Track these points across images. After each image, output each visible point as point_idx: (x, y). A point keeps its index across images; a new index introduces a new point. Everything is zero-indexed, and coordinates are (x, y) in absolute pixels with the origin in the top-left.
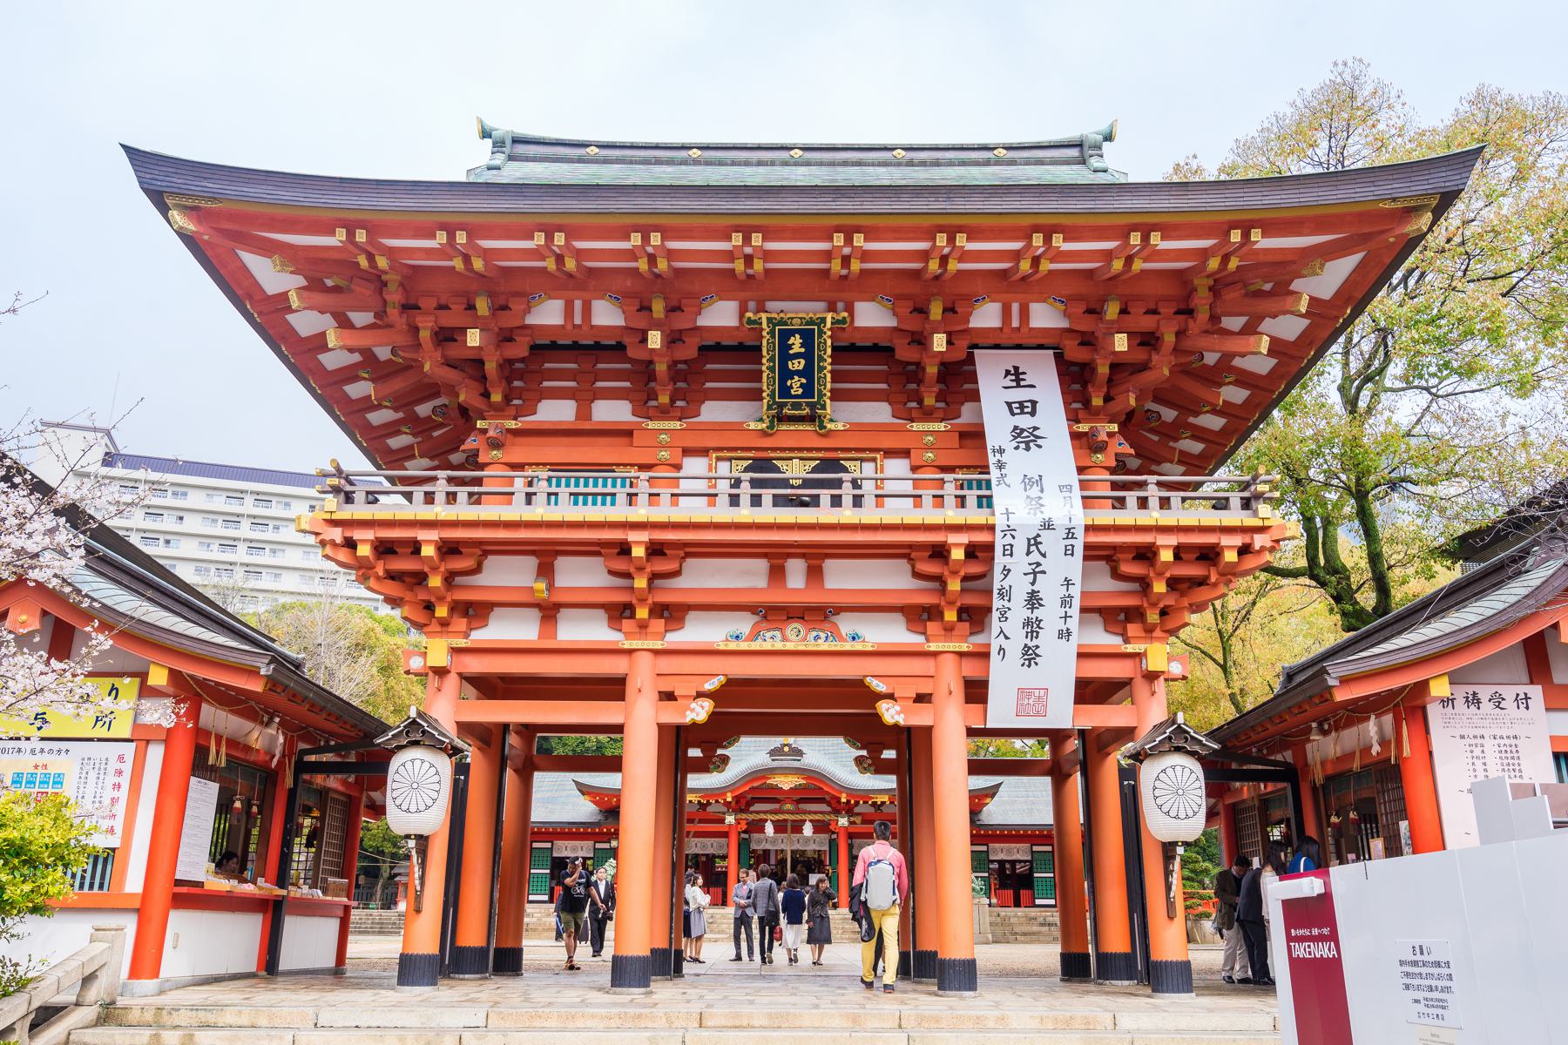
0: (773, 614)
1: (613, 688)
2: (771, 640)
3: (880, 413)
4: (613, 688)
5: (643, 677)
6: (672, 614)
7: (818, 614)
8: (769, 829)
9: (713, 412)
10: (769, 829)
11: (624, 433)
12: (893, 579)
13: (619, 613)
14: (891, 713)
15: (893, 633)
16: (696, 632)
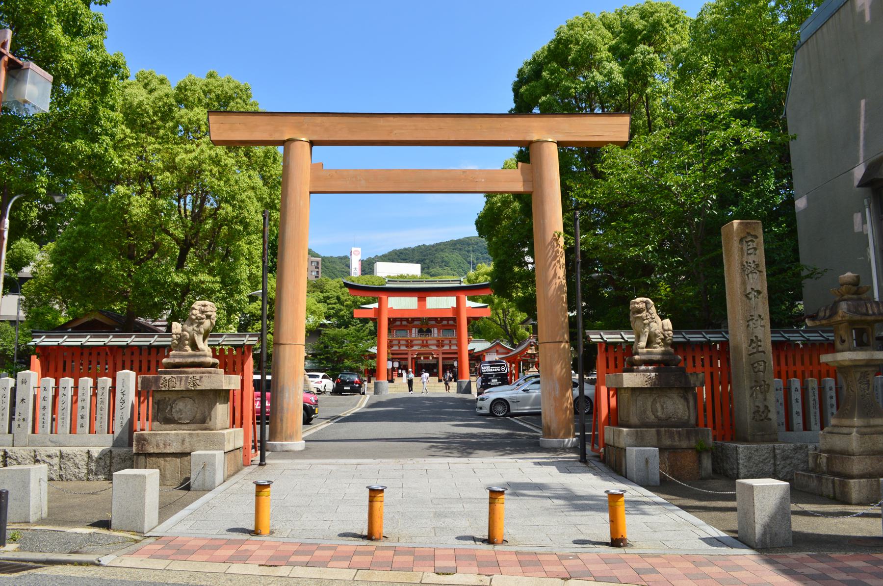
0: (423, 346)
1: (406, 354)
2: (422, 349)
3: (433, 323)
4: (406, 354)
5: (410, 354)
6: (412, 346)
7: (427, 346)
8: (422, 358)
9: (416, 323)
10: (422, 358)
11: (406, 326)
12: (435, 342)
13: (407, 346)
14: (435, 356)
15: (434, 348)
16: (415, 348)
